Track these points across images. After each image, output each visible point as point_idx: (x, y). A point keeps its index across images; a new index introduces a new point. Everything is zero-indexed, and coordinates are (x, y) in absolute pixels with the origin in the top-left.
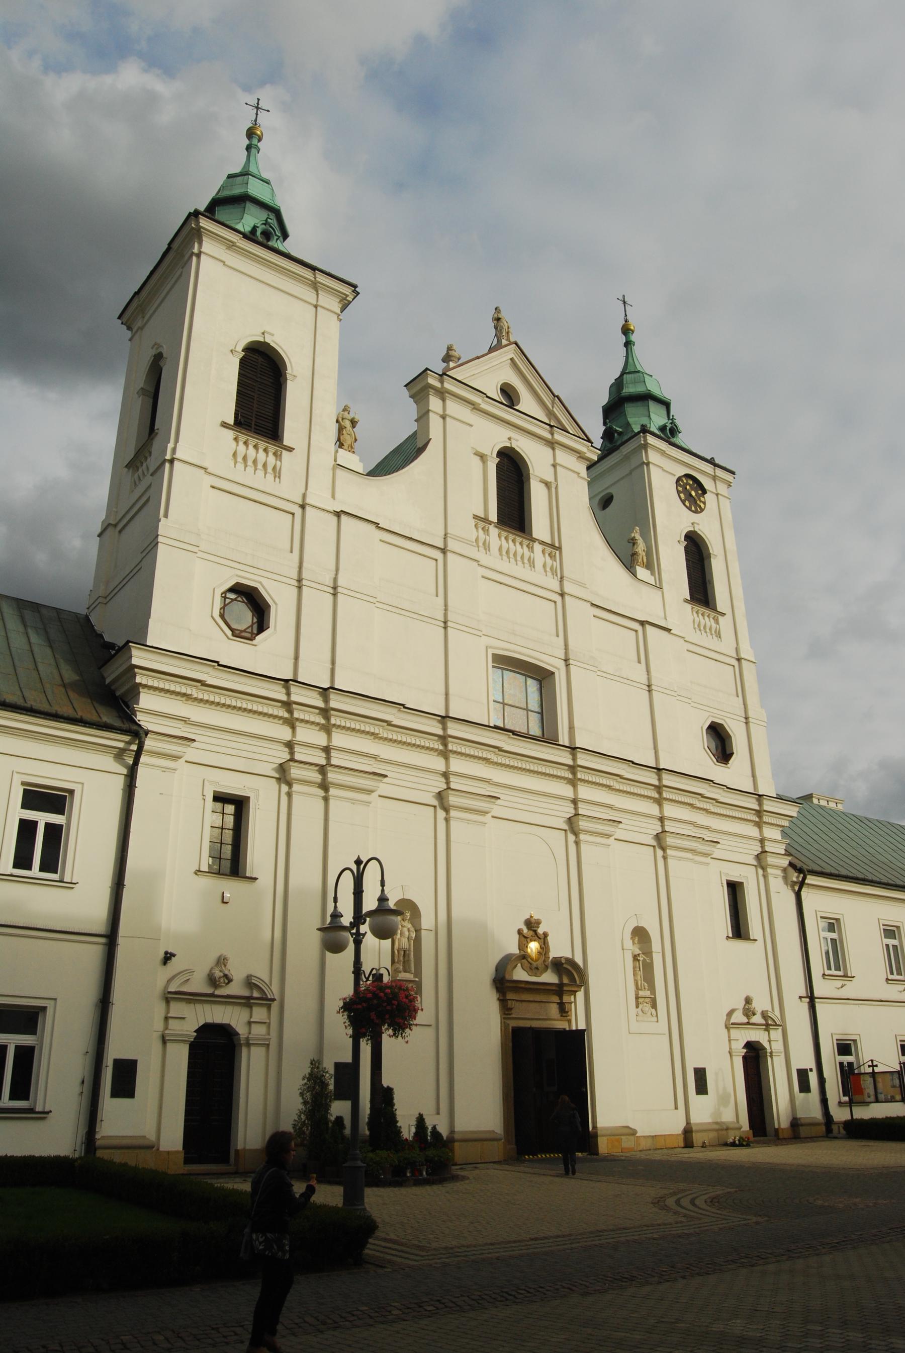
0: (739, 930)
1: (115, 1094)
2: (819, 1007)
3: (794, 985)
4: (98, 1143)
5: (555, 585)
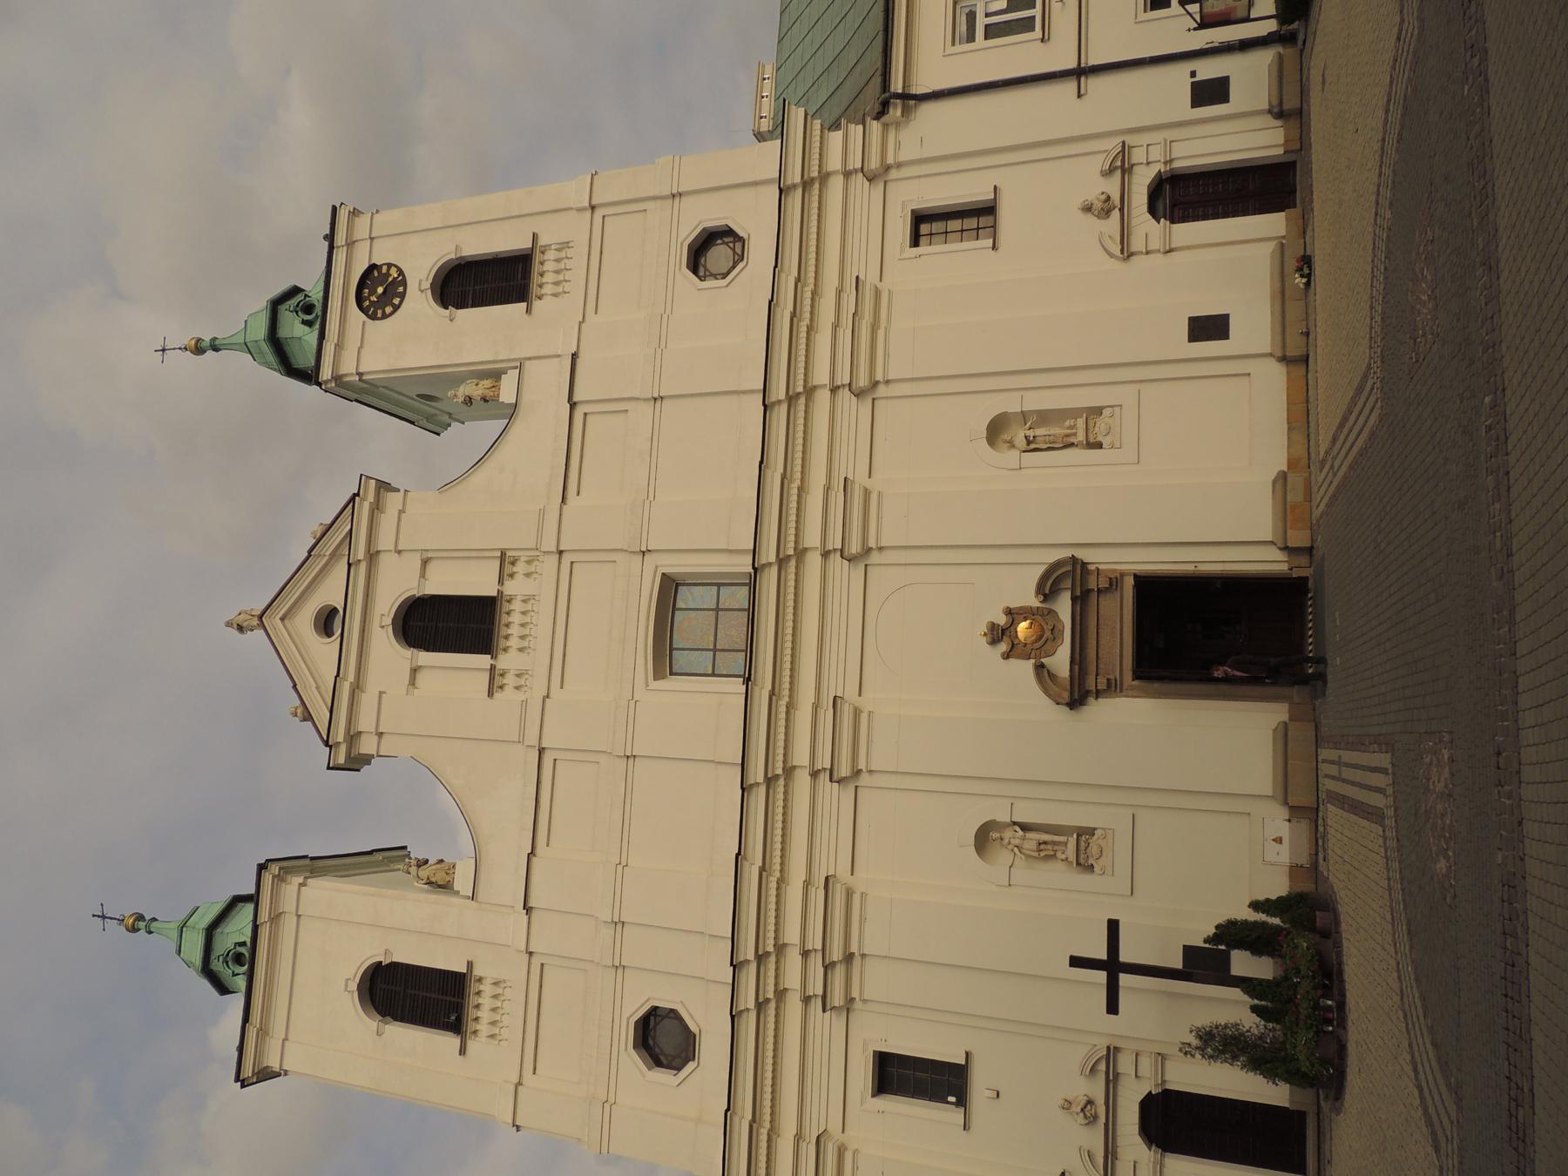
0: (980, 216)
2: (1094, 59)
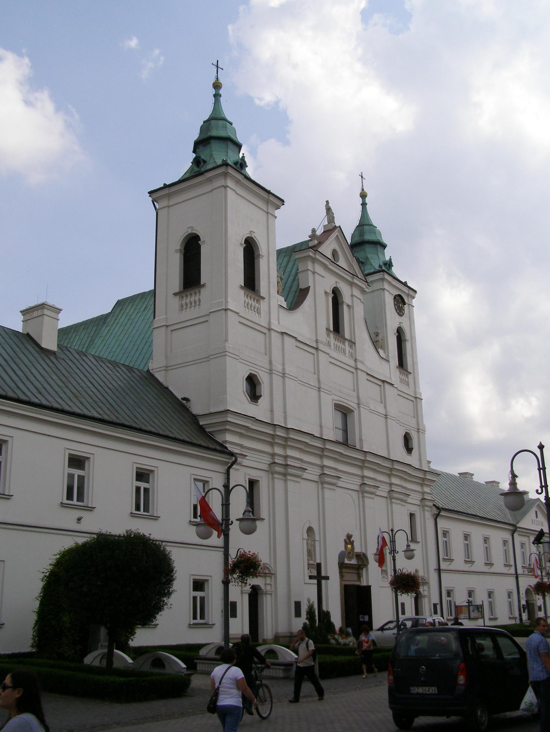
1: (231, 617)
2: (442, 575)
3: (433, 565)
4: (230, 636)
5: (352, 363)
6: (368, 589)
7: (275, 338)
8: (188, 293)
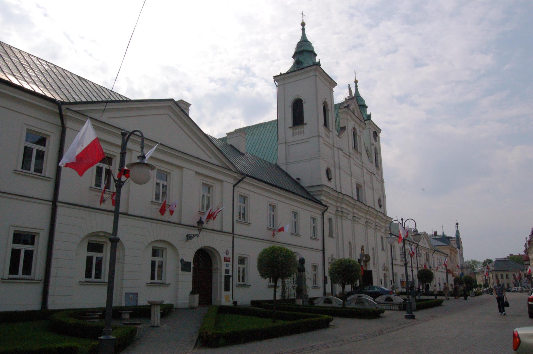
3: (390, 262)
5: (361, 164)
6: (371, 272)
7: (336, 149)
8: (297, 127)
